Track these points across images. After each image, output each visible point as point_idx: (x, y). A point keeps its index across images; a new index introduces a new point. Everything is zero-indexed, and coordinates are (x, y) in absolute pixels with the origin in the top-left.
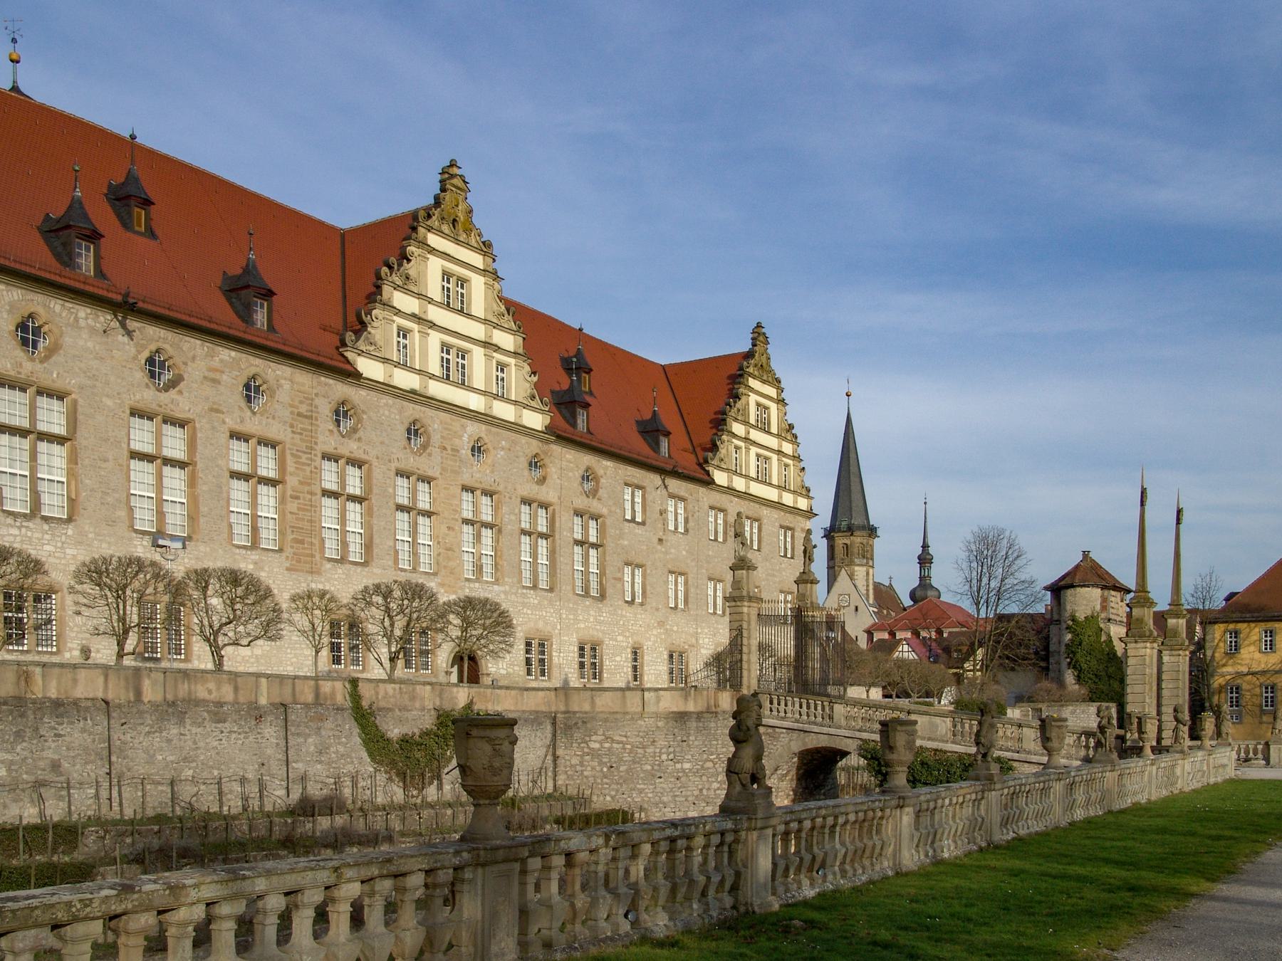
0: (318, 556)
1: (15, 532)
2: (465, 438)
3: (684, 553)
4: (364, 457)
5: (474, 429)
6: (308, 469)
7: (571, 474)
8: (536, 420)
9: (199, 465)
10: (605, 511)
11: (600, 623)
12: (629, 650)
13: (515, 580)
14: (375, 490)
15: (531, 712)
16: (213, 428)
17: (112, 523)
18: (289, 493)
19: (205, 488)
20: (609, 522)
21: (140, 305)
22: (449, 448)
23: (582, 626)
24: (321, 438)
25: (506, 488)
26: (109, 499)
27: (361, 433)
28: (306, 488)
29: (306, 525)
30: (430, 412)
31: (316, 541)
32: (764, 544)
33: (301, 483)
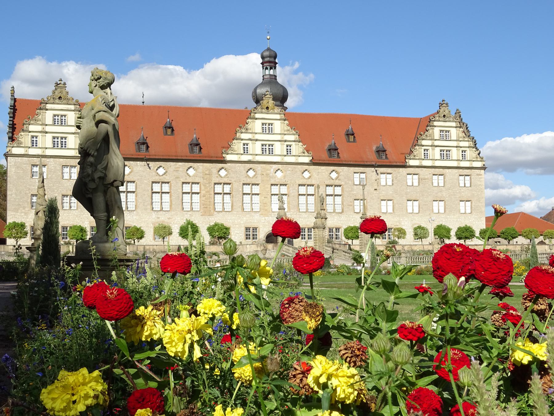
0: (212, 211)
2: (272, 170)
3: (391, 192)
4: (229, 182)
6: (209, 188)
7: (323, 174)
9: (172, 192)
10: (342, 183)
13: (295, 210)
14: (234, 190)
16: (177, 182)
17: (146, 209)
18: (202, 195)
19: (174, 198)
20: (345, 187)
22: (265, 174)
23: (330, 222)
24: (213, 179)
25: (291, 182)
26: (146, 204)
28: (208, 193)
31: (212, 207)
32: (446, 184)
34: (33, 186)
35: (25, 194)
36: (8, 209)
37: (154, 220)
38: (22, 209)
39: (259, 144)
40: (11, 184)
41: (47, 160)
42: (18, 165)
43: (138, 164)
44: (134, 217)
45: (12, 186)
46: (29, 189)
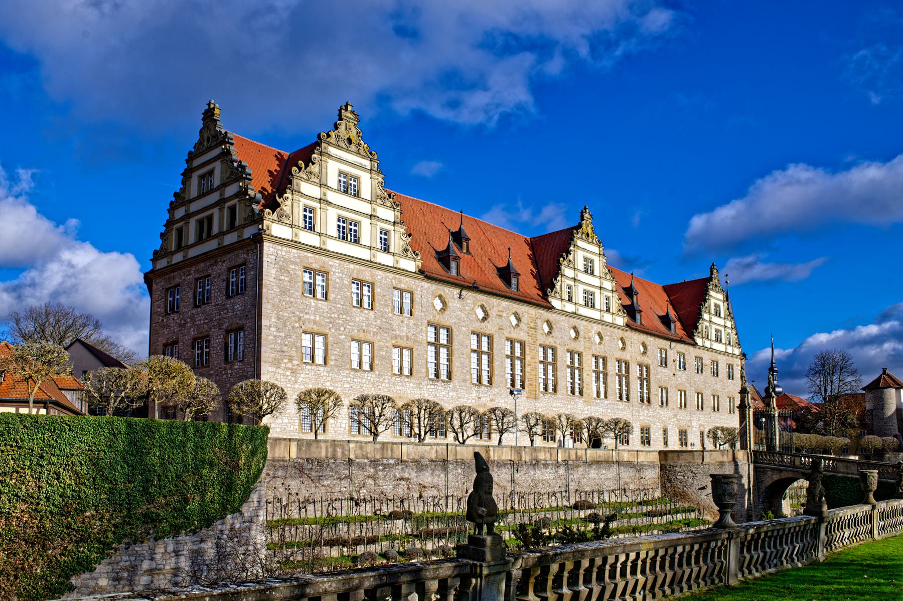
1: (433, 387)
5: (597, 328)
8: (621, 320)
10: (650, 362)
11: (650, 416)
12: (662, 430)
15: (651, 462)
17: (465, 381)
21: (481, 288)
26: (464, 371)
27: (553, 334)
28: (533, 361)
29: (533, 377)
30: (580, 322)
33: (532, 358)
34: (307, 313)
35: (293, 328)
36: (263, 359)
37: (474, 401)
38: (286, 361)
39: (581, 288)
40: (268, 302)
41: (330, 263)
42: (281, 263)
43: (456, 297)
44: (451, 394)
45: (270, 306)
46: (300, 318)
